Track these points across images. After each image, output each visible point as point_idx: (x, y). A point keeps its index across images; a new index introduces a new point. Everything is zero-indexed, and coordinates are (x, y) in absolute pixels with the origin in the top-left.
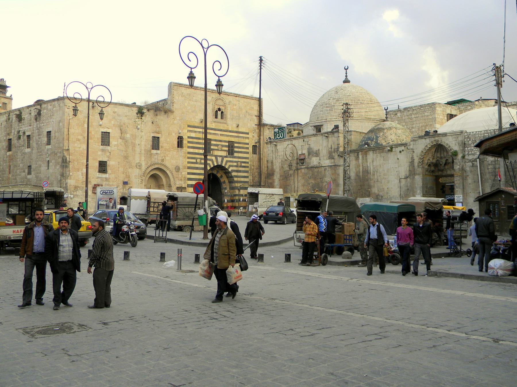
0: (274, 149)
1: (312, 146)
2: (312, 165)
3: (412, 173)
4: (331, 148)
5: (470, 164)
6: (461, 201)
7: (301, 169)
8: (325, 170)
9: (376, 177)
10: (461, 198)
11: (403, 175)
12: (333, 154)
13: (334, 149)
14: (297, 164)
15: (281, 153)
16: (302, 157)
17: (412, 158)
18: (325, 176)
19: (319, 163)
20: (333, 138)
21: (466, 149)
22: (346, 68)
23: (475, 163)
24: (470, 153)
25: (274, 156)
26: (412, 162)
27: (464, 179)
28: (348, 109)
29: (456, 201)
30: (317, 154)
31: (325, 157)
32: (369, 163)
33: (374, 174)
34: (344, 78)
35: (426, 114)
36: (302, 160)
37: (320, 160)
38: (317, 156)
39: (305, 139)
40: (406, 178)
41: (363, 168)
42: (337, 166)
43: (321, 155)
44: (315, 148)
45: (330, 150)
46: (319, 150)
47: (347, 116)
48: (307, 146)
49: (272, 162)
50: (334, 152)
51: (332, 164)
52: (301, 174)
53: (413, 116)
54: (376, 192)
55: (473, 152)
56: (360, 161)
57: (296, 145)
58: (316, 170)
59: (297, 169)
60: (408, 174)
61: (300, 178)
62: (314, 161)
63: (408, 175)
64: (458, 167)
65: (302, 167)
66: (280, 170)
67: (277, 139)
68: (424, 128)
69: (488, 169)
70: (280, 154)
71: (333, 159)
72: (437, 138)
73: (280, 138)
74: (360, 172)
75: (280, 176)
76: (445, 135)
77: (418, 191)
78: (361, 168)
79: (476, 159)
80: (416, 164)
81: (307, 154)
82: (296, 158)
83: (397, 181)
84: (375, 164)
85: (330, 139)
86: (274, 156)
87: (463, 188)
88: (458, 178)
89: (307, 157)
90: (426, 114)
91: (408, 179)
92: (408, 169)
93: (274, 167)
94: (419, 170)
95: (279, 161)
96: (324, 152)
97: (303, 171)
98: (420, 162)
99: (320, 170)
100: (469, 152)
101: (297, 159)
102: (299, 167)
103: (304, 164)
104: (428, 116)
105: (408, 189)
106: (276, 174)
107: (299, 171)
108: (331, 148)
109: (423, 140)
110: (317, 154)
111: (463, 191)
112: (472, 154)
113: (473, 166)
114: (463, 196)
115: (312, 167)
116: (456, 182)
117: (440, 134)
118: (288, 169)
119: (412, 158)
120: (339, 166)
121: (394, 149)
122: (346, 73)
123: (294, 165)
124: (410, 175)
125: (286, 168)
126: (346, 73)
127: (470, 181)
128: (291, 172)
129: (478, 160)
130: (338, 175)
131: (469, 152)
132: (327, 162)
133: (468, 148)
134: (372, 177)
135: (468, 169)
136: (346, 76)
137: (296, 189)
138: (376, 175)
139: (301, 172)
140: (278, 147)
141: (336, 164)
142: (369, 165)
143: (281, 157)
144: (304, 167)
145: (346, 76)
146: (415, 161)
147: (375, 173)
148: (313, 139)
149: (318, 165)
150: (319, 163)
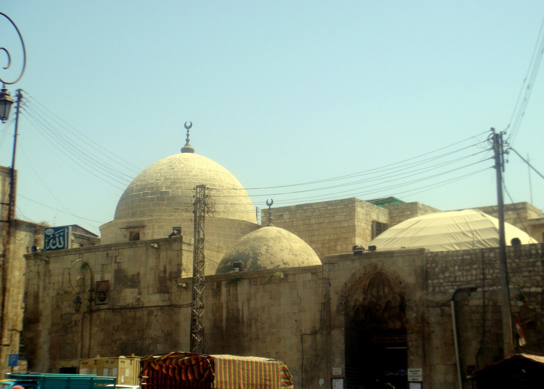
0: (42, 269)
1: (125, 266)
2: (122, 303)
3: (326, 324)
4: (165, 271)
5: (438, 310)
6: (420, 379)
7: (99, 310)
8: (150, 314)
9: (254, 330)
10: (420, 373)
11: (307, 327)
12: (169, 283)
13: (171, 273)
14: (91, 300)
15: (56, 278)
16: (103, 287)
17: (327, 296)
18: (149, 325)
19: (138, 300)
21: (430, 282)
22: (188, 125)
23: (446, 308)
24: (437, 289)
25: (41, 284)
26: (326, 305)
27: (426, 337)
28: (205, 196)
29: (410, 379)
31: (151, 290)
32: (240, 304)
33: (250, 325)
34: (183, 145)
35: (337, 218)
36: (100, 293)
37: (140, 293)
38: (132, 287)
39: (110, 252)
40: (314, 333)
41: (228, 311)
42: (176, 306)
43: (143, 284)
44: (131, 269)
45: (162, 275)
46: (138, 274)
47: (204, 211)
48: (114, 266)
51: (165, 304)
53: (313, 221)
55: (442, 289)
56: (224, 298)
57: (92, 262)
58: (130, 314)
59: (91, 311)
60: (318, 326)
61: (95, 329)
62: (129, 296)
63: (318, 328)
64: (415, 315)
65: (102, 307)
66: (53, 312)
67: (50, 249)
68: (333, 244)
69: (471, 320)
70: (54, 279)
72: (374, 260)
73: (57, 248)
74: (221, 320)
75: (53, 325)
76: (390, 254)
77: (338, 360)
78: (224, 311)
79: (450, 301)
80: (334, 308)
82: (88, 289)
83: (295, 340)
84: (252, 304)
85: (163, 254)
86: (41, 284)
87: (425, 356)
88: (414, 336)
89: (112, 288)
90: (337, 218)
91: (318, 336)
92: (318, 316)
93: (41, 306)
94: (341, 319)
95: (52, 293)
96: (149, 280)
97: (103, 314)
98: (341, 304)
99: (139, 313)
100: (434, 287)
101: (91, 290)
102: (94, 307)
103: (106, 302)
104: (340, 222)
105: (317, 356)
106: (43, 319)
107: (95, 315)
108: (165, 271)
109: (349, 263)
110: (134, 282)
111: (425, 361)
112: (440, 292)
113: (443, 314)
114: (424, 371)
116: (410, 344)
117: (381, 253)
118: (71, 310)
119: (327, 296)
120: (180, 307)
121: (291, 278)
122: (188, 135)
123: (85, 303)
124: (321, 328)
125: (67, 308)
126: (188, 135)
127: (436, 342)
128: (77, 317)
129: (452, 303)
130: (178, 325)
131: (434, 287)
132: (153, 299)
133: (432, 280)
134: (245, 331)
135: (433, 319)
136: (188, 140)
137: (86, 351)
138: (253, 327)
140: (52, 266)
141: (174, 302)
142: (240, 307)
143: (56, 287)
144: (106, 307)
145: (188, 140)
146: (332, 302)
148: (128, 252)
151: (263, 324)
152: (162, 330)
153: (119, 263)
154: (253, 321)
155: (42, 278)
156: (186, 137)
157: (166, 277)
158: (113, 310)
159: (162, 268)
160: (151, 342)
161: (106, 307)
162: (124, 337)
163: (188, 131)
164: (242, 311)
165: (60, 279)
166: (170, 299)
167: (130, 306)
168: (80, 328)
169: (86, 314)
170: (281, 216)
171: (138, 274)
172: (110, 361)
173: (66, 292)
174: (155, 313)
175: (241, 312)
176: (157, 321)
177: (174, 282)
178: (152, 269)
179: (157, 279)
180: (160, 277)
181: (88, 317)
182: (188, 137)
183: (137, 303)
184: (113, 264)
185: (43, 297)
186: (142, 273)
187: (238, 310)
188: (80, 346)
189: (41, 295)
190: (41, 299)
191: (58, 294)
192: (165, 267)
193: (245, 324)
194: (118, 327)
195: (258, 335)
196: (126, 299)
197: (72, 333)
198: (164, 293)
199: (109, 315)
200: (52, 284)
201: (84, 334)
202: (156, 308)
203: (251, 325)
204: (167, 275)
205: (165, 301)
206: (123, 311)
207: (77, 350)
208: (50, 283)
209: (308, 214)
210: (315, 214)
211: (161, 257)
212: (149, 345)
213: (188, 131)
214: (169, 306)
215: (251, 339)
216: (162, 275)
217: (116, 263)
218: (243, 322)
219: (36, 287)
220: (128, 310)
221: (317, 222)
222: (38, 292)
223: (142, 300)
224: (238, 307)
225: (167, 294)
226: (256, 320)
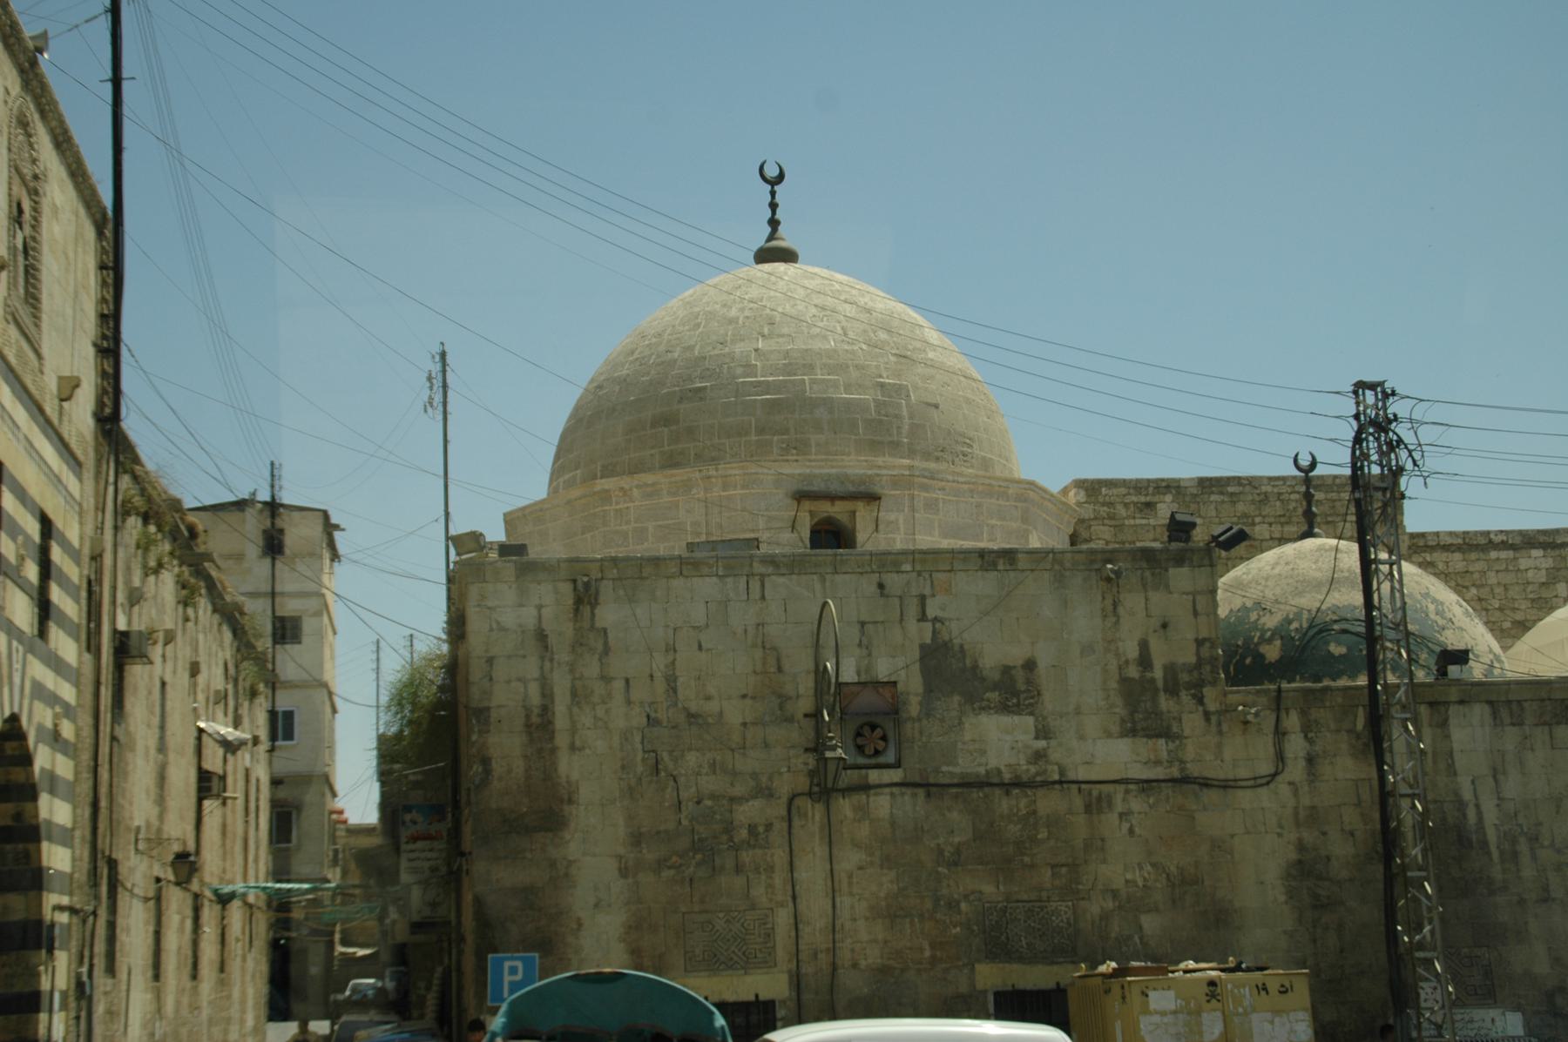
2: (965, 765)
4: (1145, 661)
7: (866, 788)
8: (1095, 807)
9: (1528, 872)
13: (1170, 669)
20: (1156, 597)
22: (772, 172)
25: (561, 684)
30: (1015, 690)
32: (1465, 783)
37: (1043, 732)
39: (894, 581)
42: (1206, 783)
44: (994, 649)
45: (1133, 672)
46: (1030, 665)
49: (540, 727)
50: (1172, 689)
51: (1159, 773)
52: (864, 831)
54: (1542, 967)
61: (849, 859)
62: (998, 740)
65: (874, 776)
71: (1167, 734)
75: (637, 839)
81: (911, 683)
84: (1512, 786)
85: (1132, 601)
89: (914, 708)
93: (568, 767)
96: (1082, 688)
97: (882, 804)
99: (1048, 803)
103: (890, 757)
107: (845, 806)
108: (1145, 661)
115: (969, 784)
122: (773, 206)
126: (773, 206)
134: (1497, 873)
136: (774, 223)
138: (1525, 858)
139: (863, 812)
141: (1194, 770)
142: (1467, 795)
145: (774, 223)
147: (1523, 847)
149: (1028, 770)
150: (1039, 756)
151: (1559, 851)
152: (1153, 865)
153: (936, 620)
154: (1522, 840)
155: (563, 656)
156: (769, 214)
157: (1153, 681)
158: (928, 787)
159: (1132, 651)
160: (1110, 904)
161: (895, 775)
162: (988, 889)
163: (773, 194)
164: (1477, 806)
165: (660, 662)
166: (1175, 759)
167: (1007, 777)
168: (779, 856)
169: (804, 803)
170: (1149, 506)
171: (1030, 665)
172: (1274, 987)
173: (692, 717)
174: (1119, 806)
175: (1471, 814)
176: (1131, 831)
177: (1185, 697)
178: (1087, 649)
179: (1114, 685)
180: (1124, 680)
181: (816, 812)
182: (774, 212)
183: (1033, 769)
184: (912, 625)
185: (573, 731)
186: (1043, 664)
187: (1461, 805)
188: (783, 918)
189: (561, 722)
190: (562, 740)
191: (652, 721)
192: (1144, 646)
193: (1495, 854)
194: (958, 852)
195: (1546, 889)
196: (983, 752)
197: (738, 869)
198: (1149, 737)
199: (911, 806)
200: (619, 685)
201: (802, 875)
202: (1121, 788)
203: (1515, 855)
204: (1158, 674)
205: (1158, 762)
206: (976, 794)
207: (769, 935)
208: (606, 679)
209: (1241, 507)
210: (1267, 510)
211: (1121, 610)
212: (1105, 917)
213: (773, 194)
214: (1173, 780)
215: (1521, 902)
216: (1133, 672)
217: (923, 617)
218: (1484, 844)
219: (534, 691)
220: (998, 792)
221: (1277, 535)
222: (546, 710)
223: (1055, 755)
224: (1457, 794)
225: (1162, 741)
226: (1534, 839)
